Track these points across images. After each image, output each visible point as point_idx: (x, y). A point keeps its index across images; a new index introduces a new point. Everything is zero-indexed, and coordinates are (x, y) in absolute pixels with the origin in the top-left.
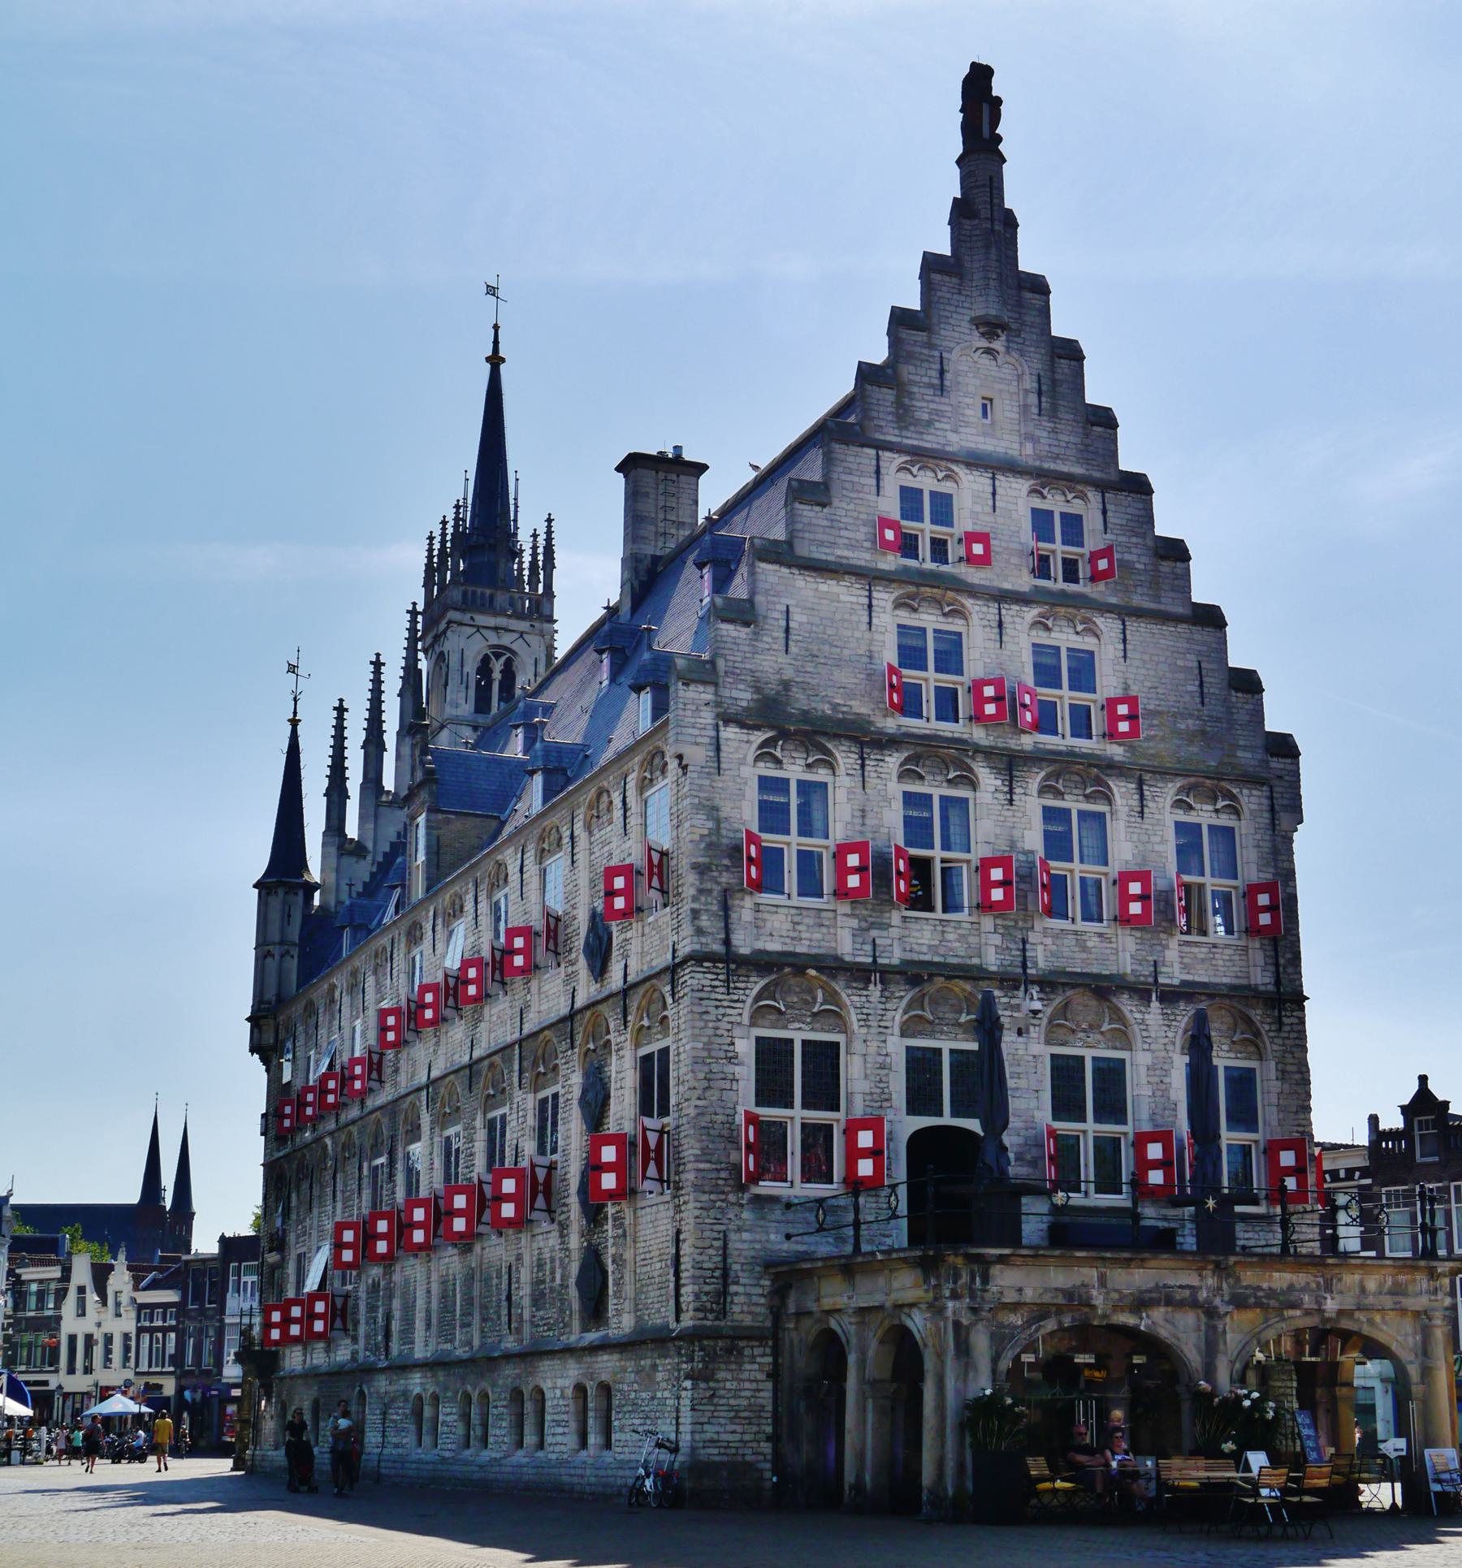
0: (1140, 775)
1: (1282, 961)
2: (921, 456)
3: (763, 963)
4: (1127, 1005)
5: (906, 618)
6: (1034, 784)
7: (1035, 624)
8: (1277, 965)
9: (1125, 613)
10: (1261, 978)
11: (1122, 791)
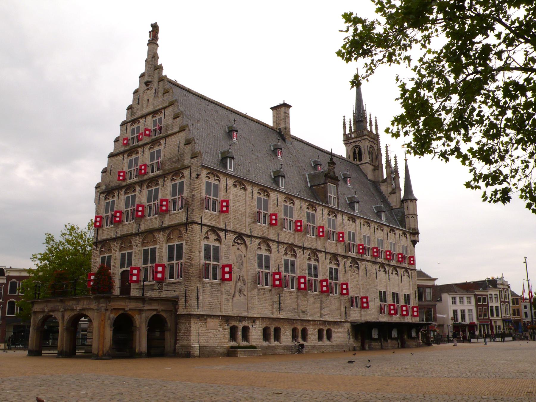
0: (163, 176)
1: (189, 213)
2: (134, 121)
3: (101, 242)
4: (156, 235)
5: (130, 158)
6: (145, 187)
7: (150, 148)
8: (187, 215)
9: (165, 137)
10: (184, 220)
11: (161, 182)
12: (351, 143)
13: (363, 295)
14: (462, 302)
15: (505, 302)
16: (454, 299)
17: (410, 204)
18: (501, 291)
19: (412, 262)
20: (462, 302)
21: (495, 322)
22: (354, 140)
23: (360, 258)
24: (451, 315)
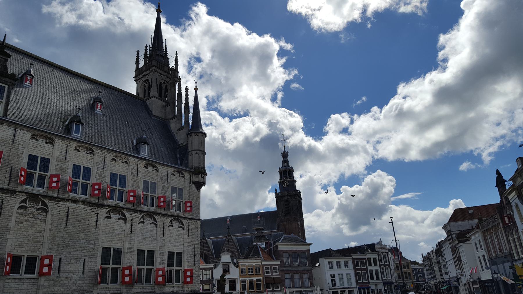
12: (140, 79)
13: (45, 253)
14: (339, 267)
15: (385, 265)
16: (330, 263)
17: (195, 139)
18: (380, 255)
19: (188, 209)
20: (339, 267)
21: (376, 285)
22: (144, 74)
23: (56, 195)
24: (329, 280)
